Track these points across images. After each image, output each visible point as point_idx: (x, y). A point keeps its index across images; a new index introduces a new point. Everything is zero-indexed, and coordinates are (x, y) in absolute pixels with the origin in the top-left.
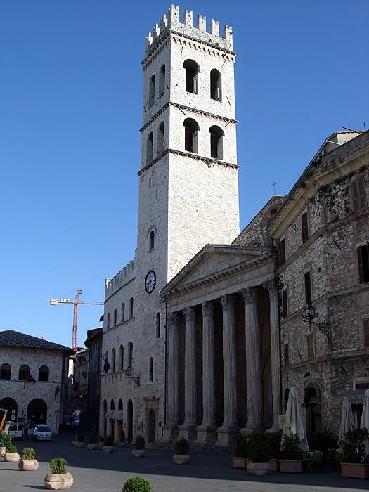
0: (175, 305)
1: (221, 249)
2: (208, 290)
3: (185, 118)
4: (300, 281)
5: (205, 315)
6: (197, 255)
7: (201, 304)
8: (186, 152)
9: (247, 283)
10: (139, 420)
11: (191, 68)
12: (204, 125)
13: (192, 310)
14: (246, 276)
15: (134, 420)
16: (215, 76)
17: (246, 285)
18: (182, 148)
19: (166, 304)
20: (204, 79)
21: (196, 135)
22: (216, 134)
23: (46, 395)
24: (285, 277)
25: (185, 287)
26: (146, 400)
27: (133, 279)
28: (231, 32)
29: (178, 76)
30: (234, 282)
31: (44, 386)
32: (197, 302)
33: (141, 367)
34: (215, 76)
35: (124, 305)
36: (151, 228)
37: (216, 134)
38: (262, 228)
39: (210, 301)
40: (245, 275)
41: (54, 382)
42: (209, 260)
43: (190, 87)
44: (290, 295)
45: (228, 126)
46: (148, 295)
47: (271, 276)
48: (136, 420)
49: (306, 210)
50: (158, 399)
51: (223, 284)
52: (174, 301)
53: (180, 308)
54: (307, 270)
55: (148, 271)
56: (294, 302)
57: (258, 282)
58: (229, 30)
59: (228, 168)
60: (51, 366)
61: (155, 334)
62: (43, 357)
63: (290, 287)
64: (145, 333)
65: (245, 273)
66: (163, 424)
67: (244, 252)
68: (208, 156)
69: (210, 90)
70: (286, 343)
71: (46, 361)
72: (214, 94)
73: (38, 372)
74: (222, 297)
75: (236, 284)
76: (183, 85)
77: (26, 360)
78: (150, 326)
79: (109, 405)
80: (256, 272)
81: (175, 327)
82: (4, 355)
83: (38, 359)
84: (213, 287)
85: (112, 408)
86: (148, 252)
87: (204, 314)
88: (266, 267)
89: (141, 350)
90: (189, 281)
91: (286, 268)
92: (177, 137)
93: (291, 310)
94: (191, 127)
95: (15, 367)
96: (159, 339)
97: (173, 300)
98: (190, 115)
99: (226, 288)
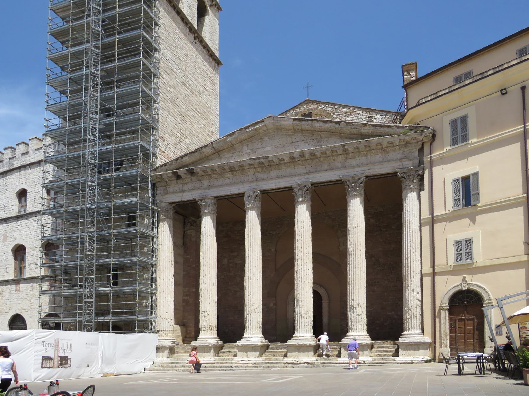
9: (357, 169)
13: (215, 201)
30: (326, 167)
32: (234, 190)
51: (300, 169)
53: (188, 196)
84: (274, 173)
90: (215, 163)
99: (308, 173)
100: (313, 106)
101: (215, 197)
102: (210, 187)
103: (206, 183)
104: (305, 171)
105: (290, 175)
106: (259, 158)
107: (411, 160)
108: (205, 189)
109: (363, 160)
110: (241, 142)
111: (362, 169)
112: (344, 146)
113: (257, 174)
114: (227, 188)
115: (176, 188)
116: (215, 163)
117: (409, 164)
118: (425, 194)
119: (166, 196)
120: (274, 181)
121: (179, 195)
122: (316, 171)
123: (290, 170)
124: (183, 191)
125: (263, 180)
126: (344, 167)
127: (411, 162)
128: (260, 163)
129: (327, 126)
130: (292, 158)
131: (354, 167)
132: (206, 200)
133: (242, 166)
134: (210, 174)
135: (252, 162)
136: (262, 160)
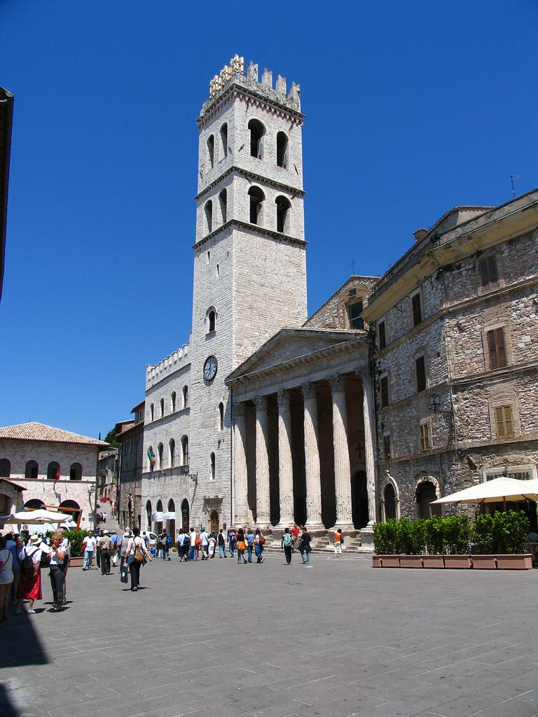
0: (242, 394)
1: (303, 332)
3: (249, 185)
4: (409, 368)
5: (281, 404)
6: (272, 339)
7: (276, 393)
8: (252, 224)
9: (335, 369)
11: (257, 129)
12: (271, 195)
14: (333, 363)
16: (282, 139)
17: (334, 372)
18: (246, 219)
20: (269, 142)
21: (261, 206)
22: (283, 205)
23: (78, 496)
24: (386, 362)
28: (299, 90)
29: (241, 136)
31: (76, 486)
32: (271, 391)
33: (198, 463)
34: (282, 139)
35: (174, 395)
37: (283, 205)
38: (338, 311)
39: (288, 390)
40: (333, 361)
41: (87, 482)
43: (255, 151)
44: (393, 381)
47: (364, 363)
48: (194, 522)
49: (418, 290)
52: (242, 389)
53: (248, 397)
54: (419, 355)
55: (207, 356)
56: (399, 390)
57: (349, 368)
58: (296, 89)
60: (84, 463)
62: (75, 453)
63: (392, 375)
64: (204, 426)
66: (228, 527)
67: (332, 335)
68: (275, 230)
69: (276, 156)
70: (386, 434)
71: (78, 458)
72: (281, 161)
73: (69, 469)
76: (248, 148)
77: (56, 456)
79: (154, 507)
80: (346, 358)
81: (242, 418)
82: (31, 451)
83: (69, 455)
85: (160, 508)
87: (279, 402)
91: (386, 353)
92: (240, 208)
93: (393, 398)
94: (256, 197)
95: (43, 465)
98: (254, 184)
100: (357, 282)
101: (263, 397)
103: (257, 384)
105: (300, 376)
110: (272, 349)
112: (321, 352)
113: (283, 376)
116: (266, 368)
121: (244, 395)
124: (246, 393)
128: (280, 368)
129: (313, 334)
131: (332, 367)
134: (257, 377)
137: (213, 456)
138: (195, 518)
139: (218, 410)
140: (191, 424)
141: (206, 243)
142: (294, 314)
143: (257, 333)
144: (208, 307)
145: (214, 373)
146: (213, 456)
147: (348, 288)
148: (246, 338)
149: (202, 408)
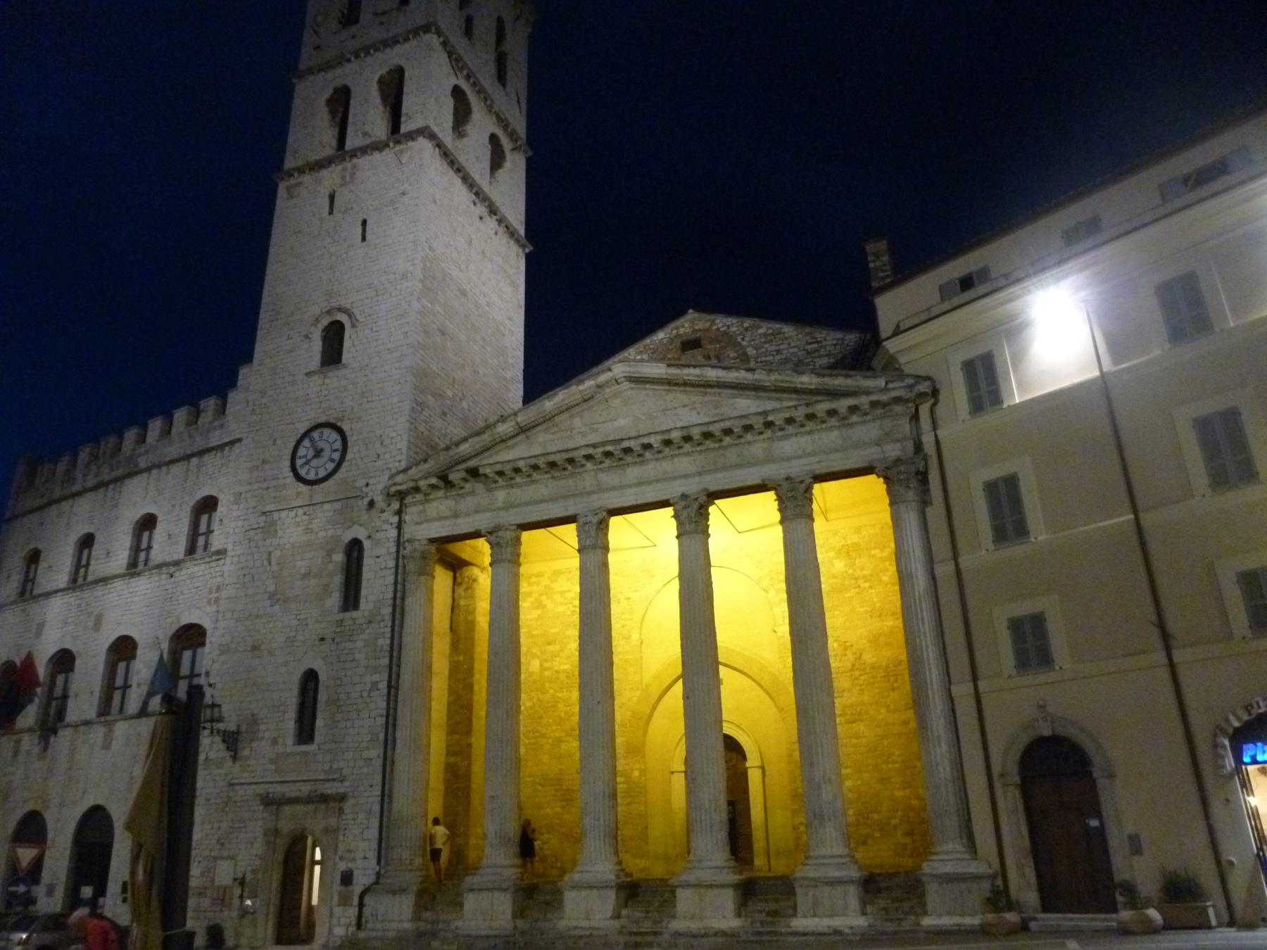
2: (609, 479)
3: (453, 81)
9: (795, 463)
10: (225, 874)
15: (195, 871)
19: (399, 513)
25: (521, 464)
26: (271, 802)
27: (221, 447)
35: (148, 522)
36: (329, 312)
42: (616, 402)
45: (515, 153)
46: (304, 488)
48: (209, 872)
50: (342, 798)
51: (684, 463)
53: (464, 526)
59: (512, 242)
61: (335, 599)
65: (787, 437)
74: (684, 496)
75: (738, 466)
78: (305, 576)
84: (633, 473)
86: (308, 374)
88: (878, 423)
89: (255, 648)
96: (355, 614)
97: (435, 504)
102: (508, 506)
103: (501, 495)
104: (694, 469)
106: (603, 444)
107: (897, 441)
108: (500, 509)
109: (805, 441)
111: (805, 461)
112: (765, 413)
113: (601, 476)
114: (543, 506)
115: (443, 508)
117: (893, 451)
118: (936, 512)
119: (424, 525)
120: (633, 490)
121: (448, 522)
122: (716, 470)
123: (666, 466)
124: (456, 515)
125: (614, 488)
126: (770, 459)
127: (898, 445)
130: (668, 443)
131: (789, 459)
132: (500, 533)
133: (571, 461)
135: (591, 451)
136: (609, 448)
137: (310, 677)
138: (215, 858)
139: (339, 557)
140: (224, 594)
141: (324, 173)
142: (505, 379)
143: (450, 393)
144: (318, 311)
145: (331, 466)
146: (310, 677)
147: (678, 336)
148: (434, 395)
149: (277, 554)
